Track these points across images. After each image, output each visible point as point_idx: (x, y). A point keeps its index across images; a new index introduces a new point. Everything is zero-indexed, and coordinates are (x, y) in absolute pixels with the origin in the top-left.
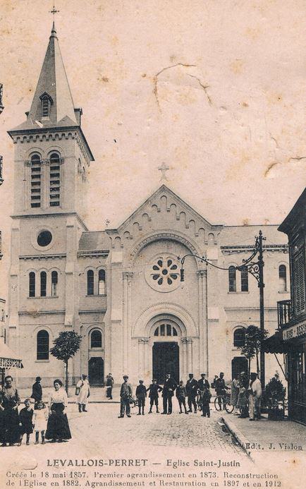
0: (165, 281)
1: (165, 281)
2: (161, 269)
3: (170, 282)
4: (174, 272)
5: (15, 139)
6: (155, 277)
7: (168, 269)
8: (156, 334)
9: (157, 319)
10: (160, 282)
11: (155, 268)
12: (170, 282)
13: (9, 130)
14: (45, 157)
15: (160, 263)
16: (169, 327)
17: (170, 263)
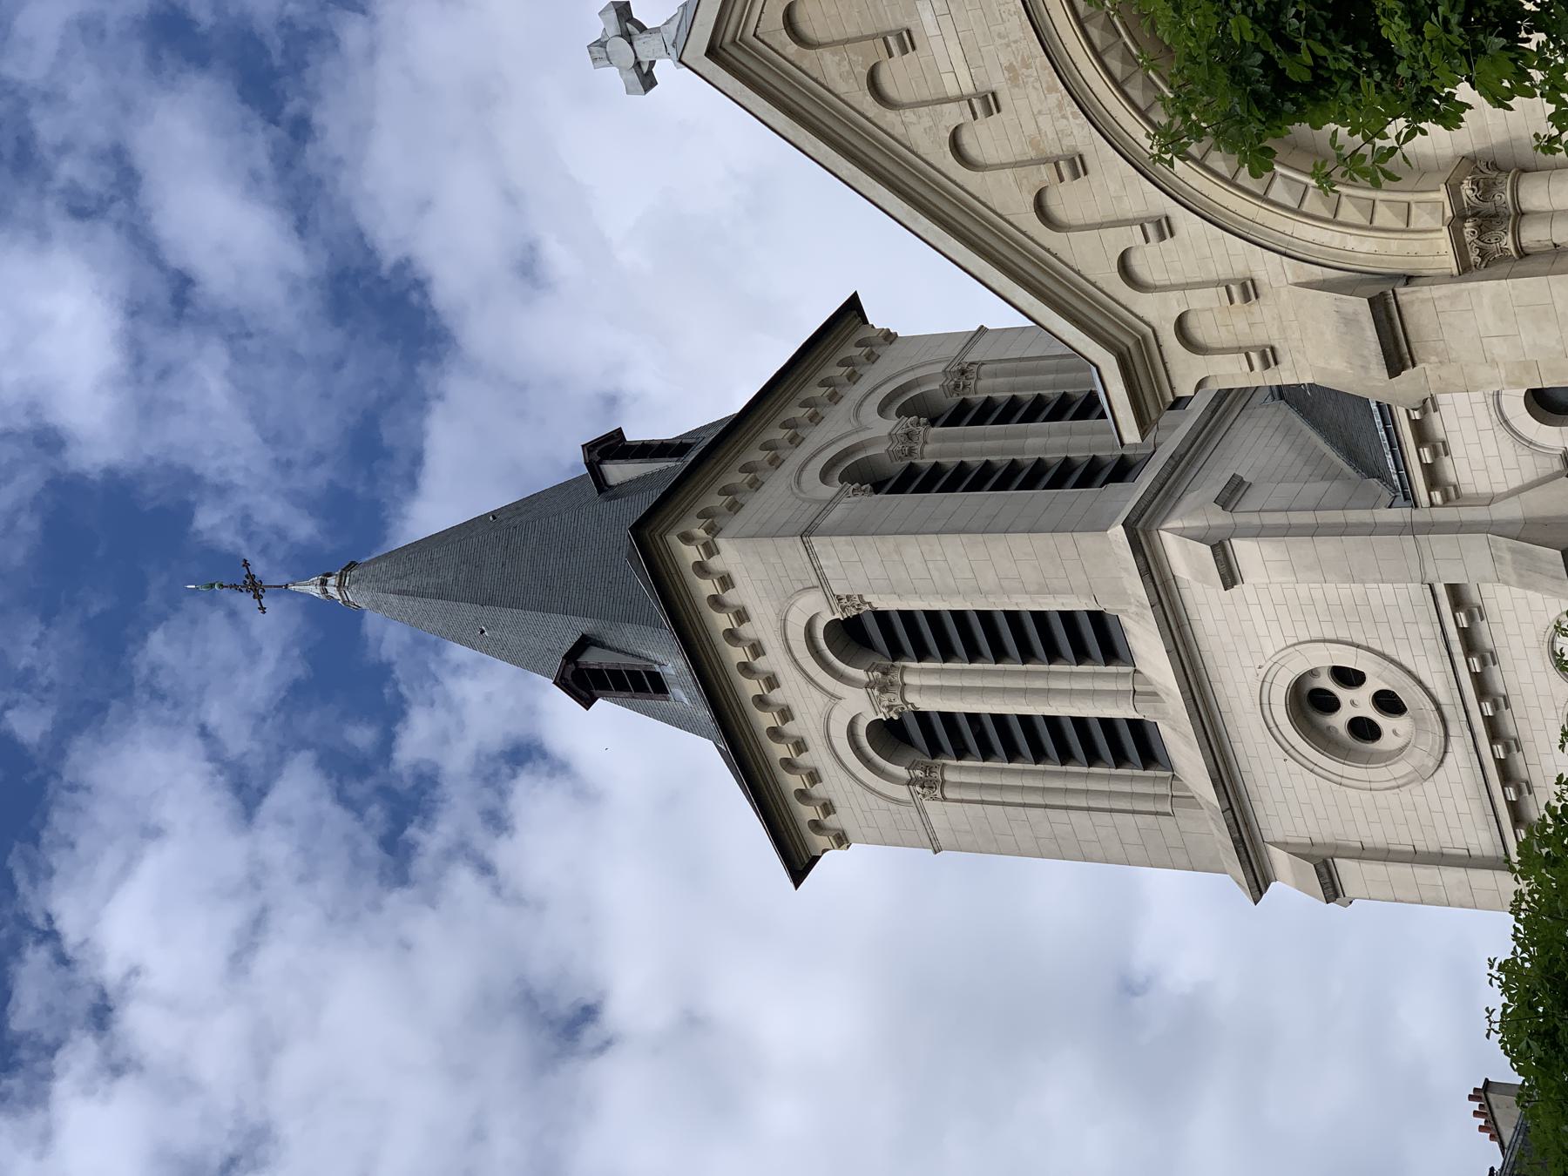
5: (821, 841)
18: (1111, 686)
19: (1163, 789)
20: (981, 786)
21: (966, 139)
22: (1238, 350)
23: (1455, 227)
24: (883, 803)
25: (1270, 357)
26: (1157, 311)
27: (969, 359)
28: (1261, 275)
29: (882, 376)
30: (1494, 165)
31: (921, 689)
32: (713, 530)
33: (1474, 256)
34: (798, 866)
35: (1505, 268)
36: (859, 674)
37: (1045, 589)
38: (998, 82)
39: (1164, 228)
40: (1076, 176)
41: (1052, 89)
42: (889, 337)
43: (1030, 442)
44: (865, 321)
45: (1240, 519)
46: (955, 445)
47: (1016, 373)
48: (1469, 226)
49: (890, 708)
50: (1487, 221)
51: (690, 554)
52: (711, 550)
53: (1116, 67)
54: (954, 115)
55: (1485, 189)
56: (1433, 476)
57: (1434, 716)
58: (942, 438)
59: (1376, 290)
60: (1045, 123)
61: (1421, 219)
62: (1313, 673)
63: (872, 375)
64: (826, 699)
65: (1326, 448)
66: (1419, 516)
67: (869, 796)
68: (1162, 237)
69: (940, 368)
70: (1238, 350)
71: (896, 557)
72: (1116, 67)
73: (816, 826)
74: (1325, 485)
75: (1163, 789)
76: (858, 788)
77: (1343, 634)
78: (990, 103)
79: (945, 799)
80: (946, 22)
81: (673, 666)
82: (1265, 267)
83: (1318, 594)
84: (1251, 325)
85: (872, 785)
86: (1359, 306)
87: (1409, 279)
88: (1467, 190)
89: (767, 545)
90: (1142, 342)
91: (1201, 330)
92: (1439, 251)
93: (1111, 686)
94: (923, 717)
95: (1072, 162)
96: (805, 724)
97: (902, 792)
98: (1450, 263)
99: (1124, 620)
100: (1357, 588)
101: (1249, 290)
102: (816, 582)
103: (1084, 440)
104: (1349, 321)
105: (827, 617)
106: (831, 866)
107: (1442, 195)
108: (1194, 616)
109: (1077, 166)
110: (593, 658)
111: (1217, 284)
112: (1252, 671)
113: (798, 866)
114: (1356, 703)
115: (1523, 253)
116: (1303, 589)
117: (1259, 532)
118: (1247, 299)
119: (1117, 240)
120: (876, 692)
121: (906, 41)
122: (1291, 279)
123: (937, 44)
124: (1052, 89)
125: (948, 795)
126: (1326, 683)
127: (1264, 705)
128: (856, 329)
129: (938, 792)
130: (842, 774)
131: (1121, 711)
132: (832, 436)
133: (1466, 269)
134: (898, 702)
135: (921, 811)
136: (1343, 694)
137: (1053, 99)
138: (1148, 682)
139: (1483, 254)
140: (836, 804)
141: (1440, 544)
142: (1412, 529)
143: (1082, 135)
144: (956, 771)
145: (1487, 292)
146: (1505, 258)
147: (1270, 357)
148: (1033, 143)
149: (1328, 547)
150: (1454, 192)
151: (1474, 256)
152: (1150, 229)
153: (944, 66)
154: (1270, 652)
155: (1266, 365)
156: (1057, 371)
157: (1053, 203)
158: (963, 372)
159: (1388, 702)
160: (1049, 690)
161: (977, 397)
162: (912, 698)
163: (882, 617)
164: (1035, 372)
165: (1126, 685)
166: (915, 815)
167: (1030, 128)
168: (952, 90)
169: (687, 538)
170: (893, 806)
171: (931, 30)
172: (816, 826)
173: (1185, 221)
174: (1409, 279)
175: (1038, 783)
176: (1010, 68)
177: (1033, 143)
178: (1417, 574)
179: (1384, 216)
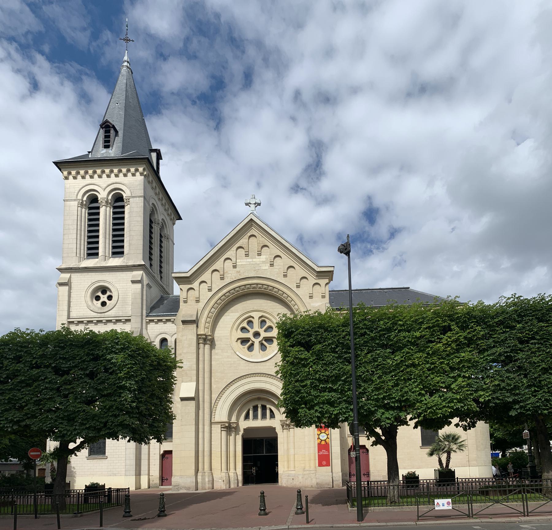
0: (257, 346)
1: (257, 346)
2: (252, 331)
3: (263, 347)
4: (269, 335)
5: (65, 173)
6: (244, 341)
7: (262, 331)
8: (247, 417)
9: (248, 398)
10: (251, 348)
11: (243, 329)
12: (263, 347)
13: (56, 160)
14: (102, 195)
15: (250, 323)
16: (264, 408)
17: (263, 322)
18: (107, 252)
19: (82, 256)
20: (81, 216)
21: (229, 261)
24: (77, 192)
25: (185, 302)
26: (195, 285)
28: (200, 304)
31: (106, 210)
32: (145, 176)
33: (199, 337)
37: (130, 245)
38: (238, 269)
39: (210, 290)
40: (221, 278)
41: (235, 278)
45: (145, 287)
48: (205, 337)
49: (102, 202)
50: (205, 340)
51: (141, 169)
52: (141, 174)
53: (237, 289)
54: (234, 260)
55: (209, 340)
56: (152, 321)
60: (230, 275)
64: (104, 187)
66: (144, 317)
67: (78, 189)
71: (138, 215)
72: (237, 289)
75: (82, 256)
76: (81, 187)
78: (235, 267)
79: (78, 207)
80: (248, 263)
81: (113, 152)
82: (201, 305)
85: (81, 190)
86: (194, 318)
87: (197, 326)
88: (210, 337)
89: (142, 187)
91: (191, 292)
92: (201, 331)
93: (107, 252)
94: (98, 208)
95: (223, 278)
98: (199, 333)
99: (122, 259)
100: (130, 304)
101: (198, 301)
102: (133, 195)
104: (192, 316)
105: (124, 195)
107: (209, 334)
108: (124, 273)
109: (222, 279)
110: (112, 132)
112: (112, 280)
114: (104, 298)
115: (199, 344)
116: (130, 294)
118: (196, 301)
119: (209, 281)
121: (247, 255)
123: (245, 260)
124: (235, 278)
127: (104, 281)
131: (101, 251)
133: (198, 335)
134: (103, 204)
135: (75, 200)
136: (106, 296)
137: (234, 277)
138: (108, 259)
139: (200, 338)
141: (139, 319)
142: (142, 315)
143: (227, 280)
144: (85, 212)
145: (195, 338)
147: (185, 302)
148: (227, 272)
149: (139, 301)
150: (210, 336)
151: (199, 337)
152: (210, 288)
153: (242, 260)
154: (116, 285)
155: (184, 301)
157: (216, 273)
159: (104, 304)
160: (106, 238)
162: (104, 207)
163: (123, 207)
165: (107, 255)
166: (73, 198)
167: (230, 272)
168: (238, 261)
169: (144, 170)
170: (76, 194)
171: (248, 260)
173: (211, 294)
174: (197, 326)
176: (240, 272)
177: (227, 272)
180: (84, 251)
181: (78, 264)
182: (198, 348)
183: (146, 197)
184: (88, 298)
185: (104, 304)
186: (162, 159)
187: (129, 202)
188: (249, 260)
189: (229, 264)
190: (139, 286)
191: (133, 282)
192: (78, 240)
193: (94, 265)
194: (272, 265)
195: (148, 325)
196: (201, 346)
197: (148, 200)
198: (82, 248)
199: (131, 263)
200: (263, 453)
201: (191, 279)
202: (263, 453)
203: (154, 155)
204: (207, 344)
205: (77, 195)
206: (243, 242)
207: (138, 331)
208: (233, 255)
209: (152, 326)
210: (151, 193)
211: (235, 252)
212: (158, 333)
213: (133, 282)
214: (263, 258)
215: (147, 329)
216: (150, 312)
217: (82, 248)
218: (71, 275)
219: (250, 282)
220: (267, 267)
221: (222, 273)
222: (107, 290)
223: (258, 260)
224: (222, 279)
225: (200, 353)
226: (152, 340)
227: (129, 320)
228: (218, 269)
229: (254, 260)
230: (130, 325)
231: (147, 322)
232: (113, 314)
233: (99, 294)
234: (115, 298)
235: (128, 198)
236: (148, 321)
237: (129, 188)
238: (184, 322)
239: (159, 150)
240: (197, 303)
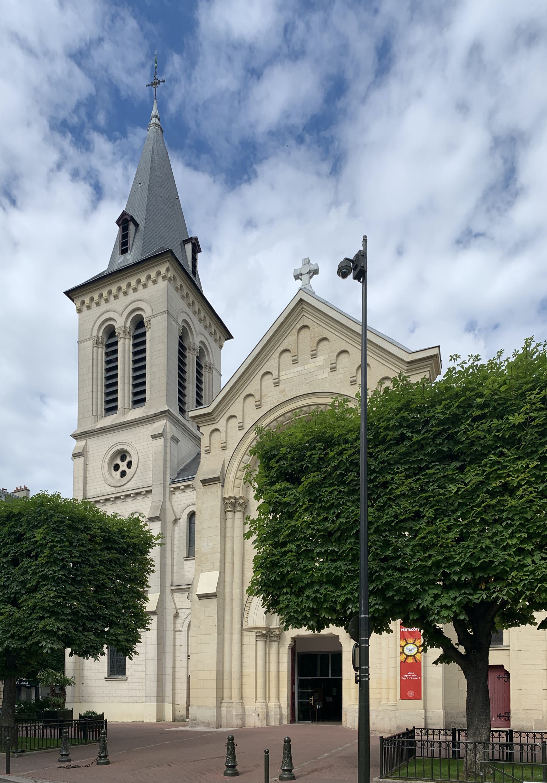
5: (79, 304)
20: (97, 359)
22: (210, 444)
23: (233, 498)
24: (91, 326)
25: (208, 452)
26: (221, 424)
27: (214, 370)
28: (227, 451)
29: (211, 344)
30: (246, 507)
31: (124, 344)
33: (226, 501)
34: (71, 294)
35: (223, 508)
36: (128, 324)
39: (241, 428)
42: (221, 347)
43: (191, 386)
44: (226, 340)
46: (191, 364)
47: (209, 384)
48: (233, 501)
49: (119, 333)
50: (234, 505)
55: (241, 505)
56: (178, 488)
57: (120, 484)
58: (193, 359)
59: (221, 478)
61: (236, 490)
62: (130, 456)
63: (211, 340)
64: (121, 312)
65: (185, 464)
67: (93, 323)
68: (239, 427)
69: (212, 361)
70: (210, 444)
73: (83, 303)
74: (176, 463)
76: (95, 319)
77: (140, 464)
79: (93, 347)
82: (229, 452)
83: (150, 459)
84: (216, 448)
85: (96, 324)
86: (217, 474)
87: (223, 486)
88: (241, 501)
90: (214, 419)
91: (216, 434)
92: (229, 493)
94: (116, 343)
96: (114, 304)
97: (95, 334)
98: (225, 496)
100: (151, 469)
101: (224, 448)
103: (191, 401)
104: (214, 472)
106: (70, 306)
107: (241, 495)
108: (145, 427)
111: (226, 441)
113: (71, 294)
115: (226, 512)
116: (151, 455)
117: (165, 446)
118: (222, 447)
120: (123, 329)
122: (226, 459)
125: (95, 348)
126: (128, 459)
128: (224, 337)
129: (95, 345)
130: (99, 314)
131: (119, 404)
132: (195, 325)
133: (224, 499)
134: (121, 336)
135: (89, 339)
138: (128, 412)
139: (227, 503)
140: (90, 311)
141: (161, 489)
142: (165, 483)
144: (101, 351)
145: (218, 504)
146: (225, 508)
147: (208, 452)
149: (161, 463)
150: (241, 498)
151: (226, 501)
152: (241, 424)
155: (206, 451)
156: (209, 396)
158: (210, 368)
161: (203, 371)
162: (122, 340)
164: (209, 390)
166: (88, 337)
170: (90, 330)
172: (83, 303)
173: (242, 433)
174: (223, 486)
175: (99, 378)
178: (154, 483)
179: (237, 482)
180: (101, 406)
181: (93, 425)
182: (224, 519)
183: (172, 312)
184: (106, 470)
185: (123, 474)
186: (200, 251)
187: (150, 324)
188: (298, 368)
189: (269, 381)
190: (161, 441)
191: (154, 437)
192: (94, 393)
193: (112, 422)
194: (333, 369)
195: (173, 495)
196: (230, 514)
197: (175, 317)
198: (99, 403)
199: (152, 412)
200: (328, 676)
201: (214, 416)
202: (328, 676)
203: (189, 247)
204: (237, 511)
205: (92, 332)
206: (289, 342)
207: (159, 505)
208: (275, 365)
209: (178, 495)
210: (180, 304)
211: (277, 360)
212: (185, 506)
213: (154, 437)
214: (320, 360)
215: (171, 502)
216: (177, 477)
217: (99, 403)
218: (86, 442)
219: (300, 403)
220: (325, 373)
221: (257, 397)
222: (127, 454)
223: (312, 365)
224: (258, 407)
225: (227, 526)
226: (178, 517)
227: (149, 492)
228: (252, 393)
229: (306, 367)
230: (151, 499)
231: (171, 491)
232: (132, 486)
233: (118, 461)
234: (134, 465)
235: (148, 319)
236: (172, 489)
237: (150, 304)
238: (205, 482)
239: (196, 239)
240: (224, 451)
